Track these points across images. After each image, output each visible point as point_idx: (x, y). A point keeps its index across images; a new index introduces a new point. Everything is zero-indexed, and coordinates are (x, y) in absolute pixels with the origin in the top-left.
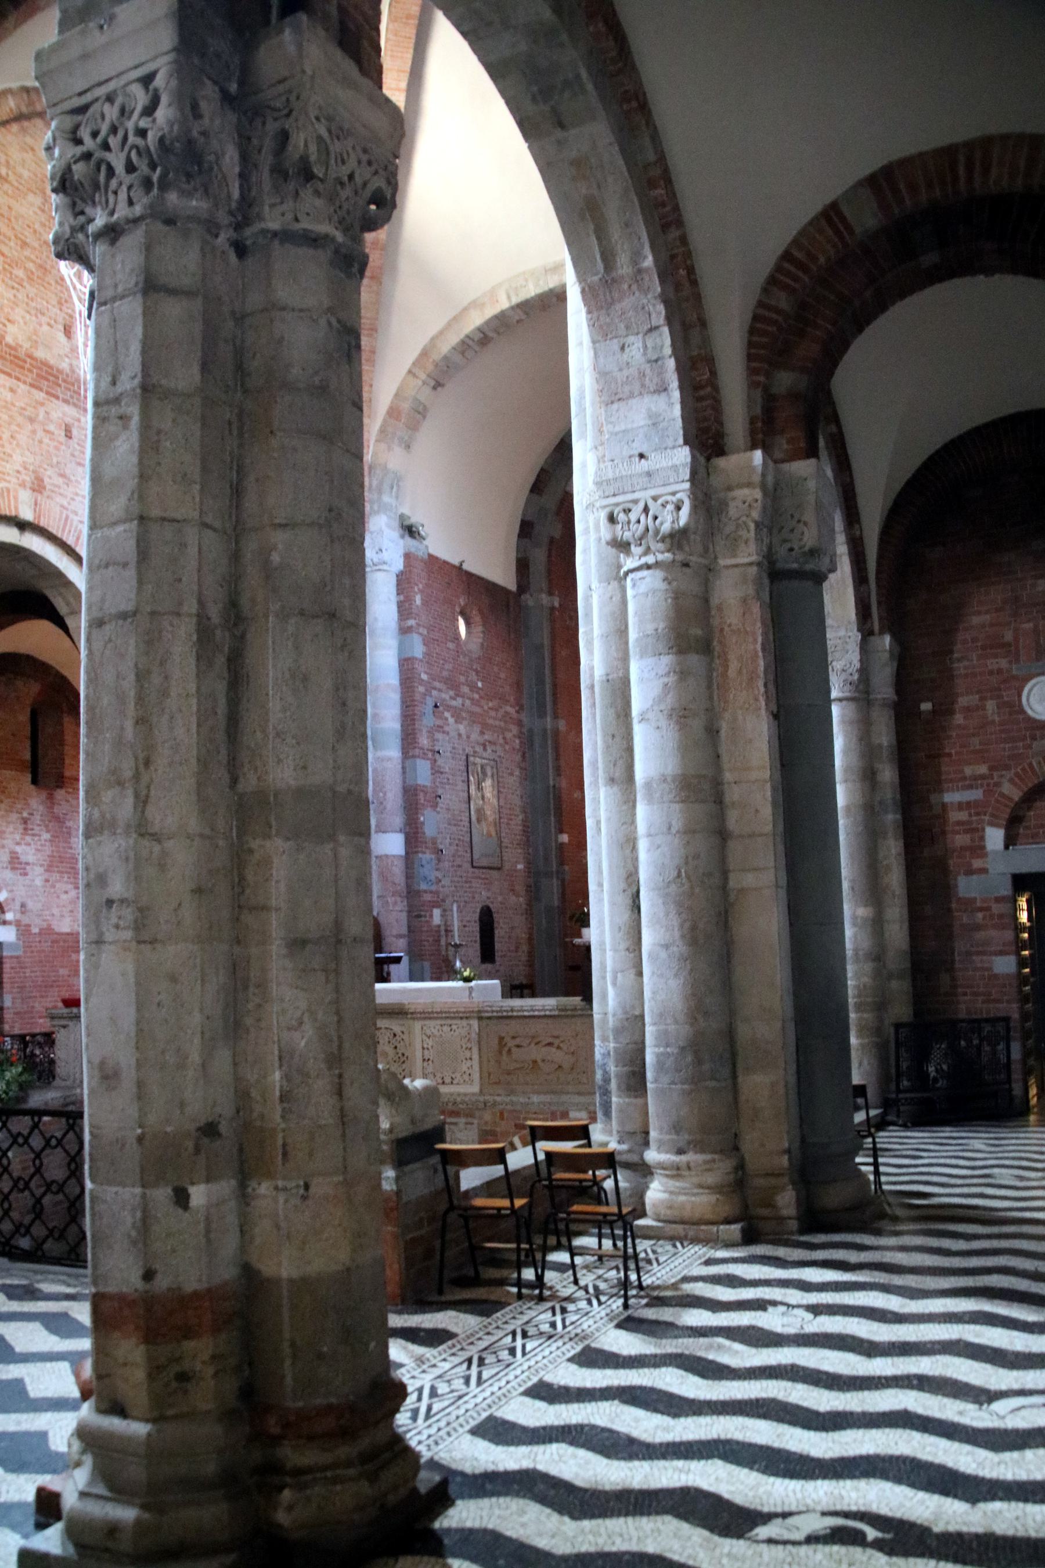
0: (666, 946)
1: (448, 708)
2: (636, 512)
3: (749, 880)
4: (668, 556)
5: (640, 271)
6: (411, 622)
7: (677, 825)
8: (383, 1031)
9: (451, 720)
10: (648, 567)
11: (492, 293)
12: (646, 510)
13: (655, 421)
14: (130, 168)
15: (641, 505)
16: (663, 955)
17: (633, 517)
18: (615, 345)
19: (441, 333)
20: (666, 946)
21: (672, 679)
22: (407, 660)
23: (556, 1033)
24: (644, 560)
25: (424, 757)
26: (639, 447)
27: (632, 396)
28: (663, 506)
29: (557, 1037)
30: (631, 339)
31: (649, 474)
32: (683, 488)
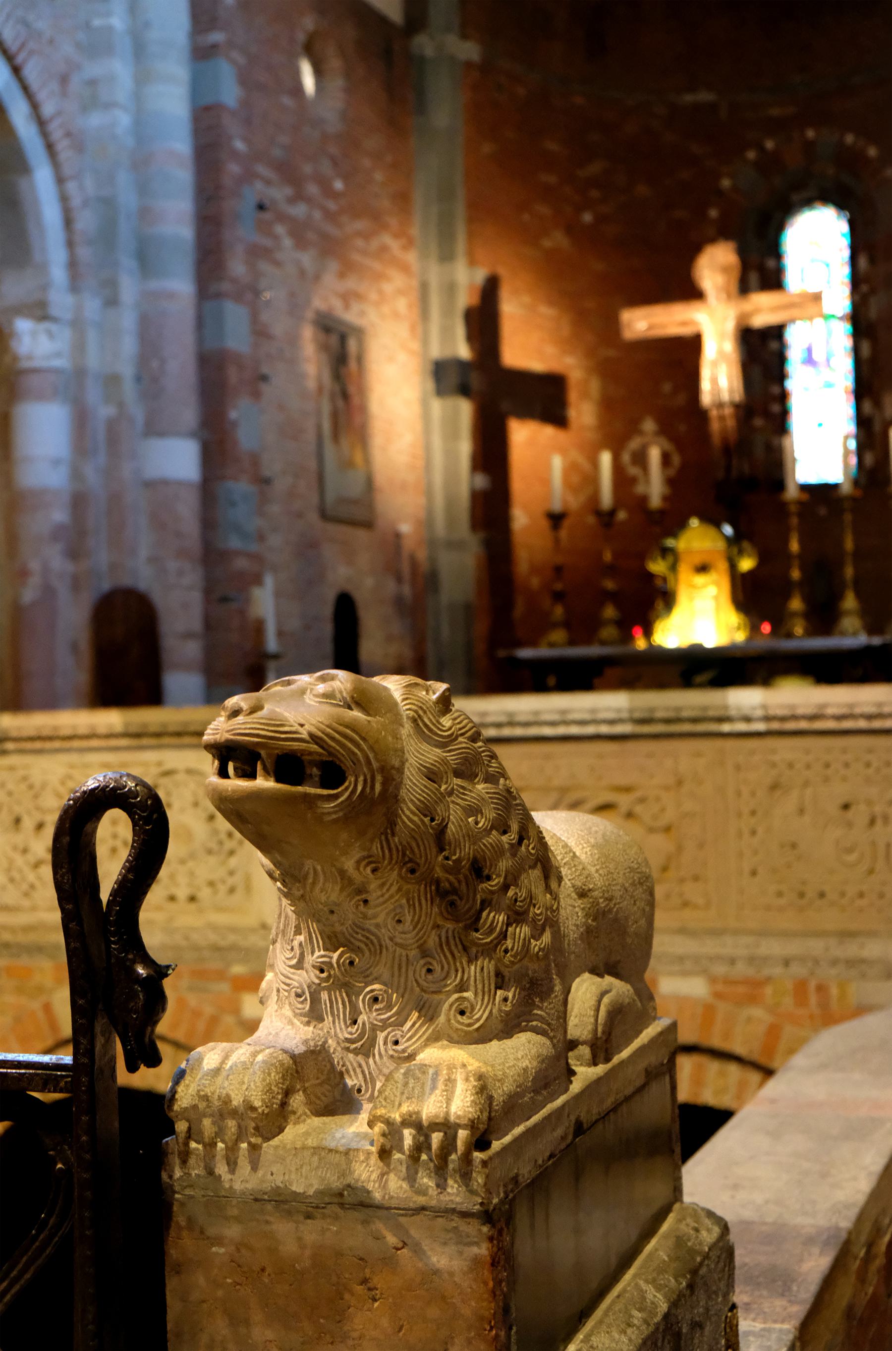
1: (282, 218)
6: (217, 37)
8: (180, 777)
9: (287, 242)
22: (207, 109)
23: (623, 781)
25: (238, 297)
29: (627, 789)
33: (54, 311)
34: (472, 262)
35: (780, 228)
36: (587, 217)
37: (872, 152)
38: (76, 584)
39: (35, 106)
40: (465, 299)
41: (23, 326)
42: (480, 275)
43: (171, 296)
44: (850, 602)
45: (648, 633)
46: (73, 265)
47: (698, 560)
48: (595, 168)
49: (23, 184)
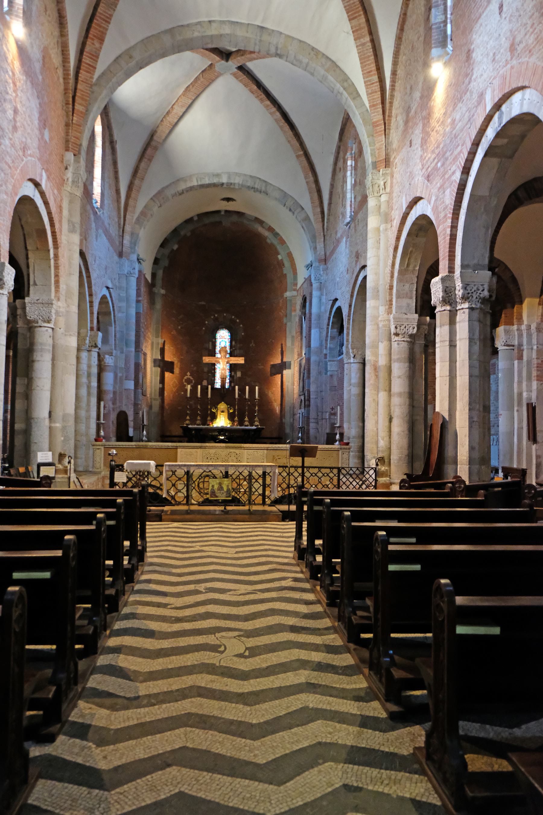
0: (403, 432)
2: (403, 326)
3: (418, 418)
4: (408, 339)
5: (414, 270)
6: (140, 299)
7: (407, 403)
10: (404, 341)
11: (191, 177)
12: (405, 327)
13: (408, 305)
14: (477, 298)
15: (404, 326)
16: (402, 433)
17: (402, 328)
18: (402, 284)
19: (167, 187)
20: (403, 432)
21: (408, 369)
24: (403, 339)
26: (404, 311)
27: (403, 298)
28: (410, 327)
30: (407, 284)
31: (407, 319)
32: (415, 324)
33: (114, 354)
34: (162, 338)
35: (216, 332)
36: (179, 327)
37: (238, 321)
38: (113, 410)
39: (114, 314)
40: (160, 346)
41: (107, 356)
42: (163, 340)
43: (132, 352)
44: (246, 419)
45: (212, 423)
46: (115, 344)
47: (221, 410)
48: (181, 317)
49: (110, 328)
